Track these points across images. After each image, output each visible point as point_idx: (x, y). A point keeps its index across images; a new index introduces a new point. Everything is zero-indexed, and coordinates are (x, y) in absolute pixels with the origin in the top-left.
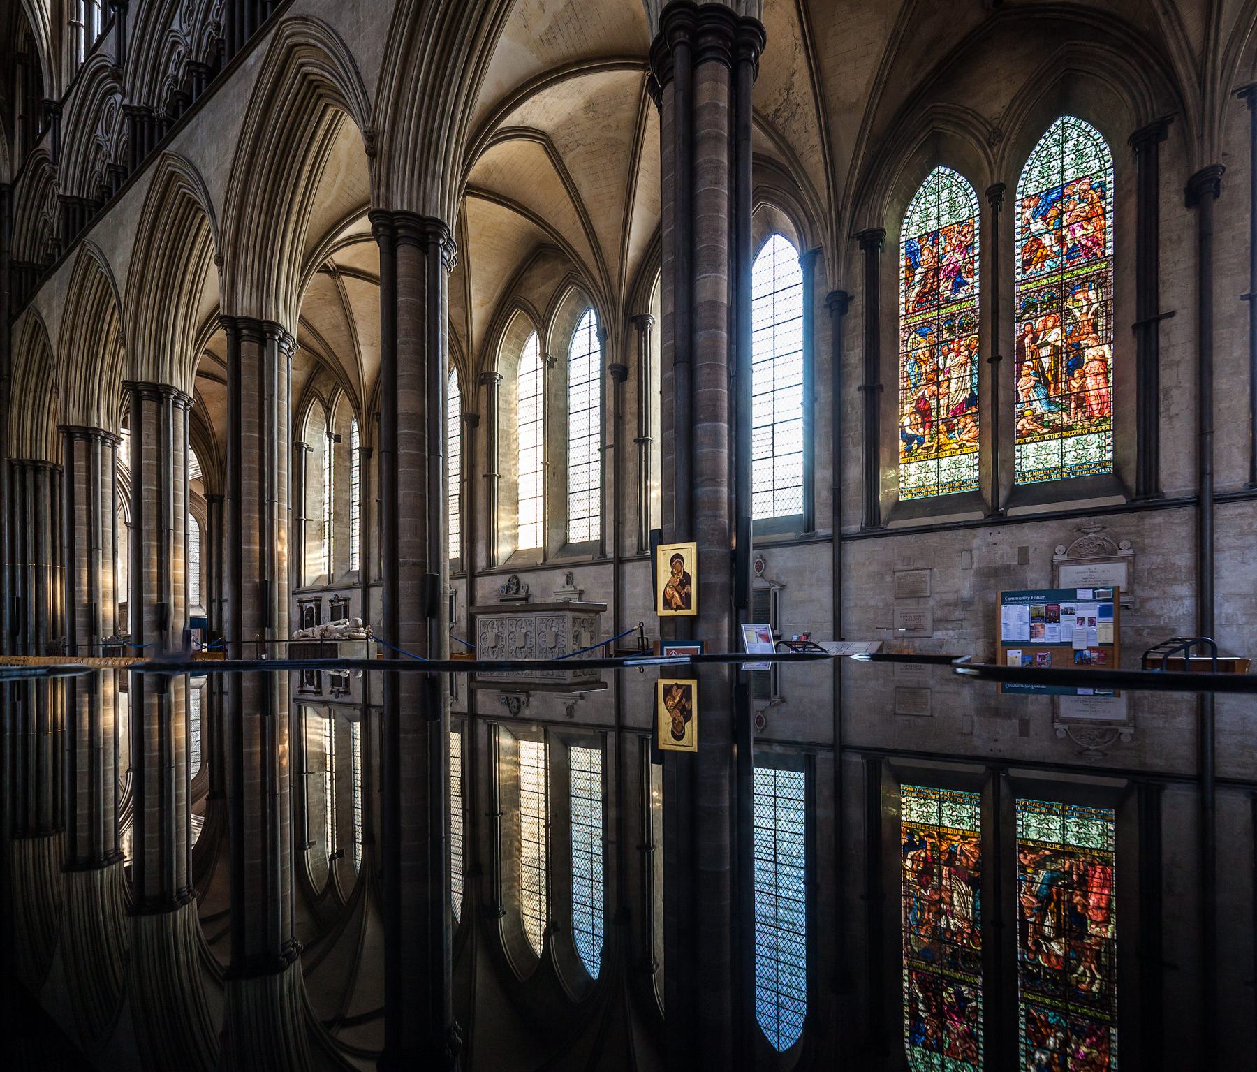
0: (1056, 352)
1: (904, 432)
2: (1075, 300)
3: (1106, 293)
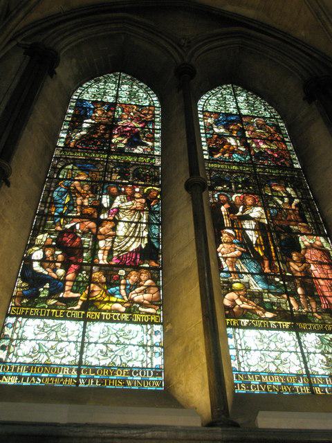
0: (260, 228)
2: (272, 191)
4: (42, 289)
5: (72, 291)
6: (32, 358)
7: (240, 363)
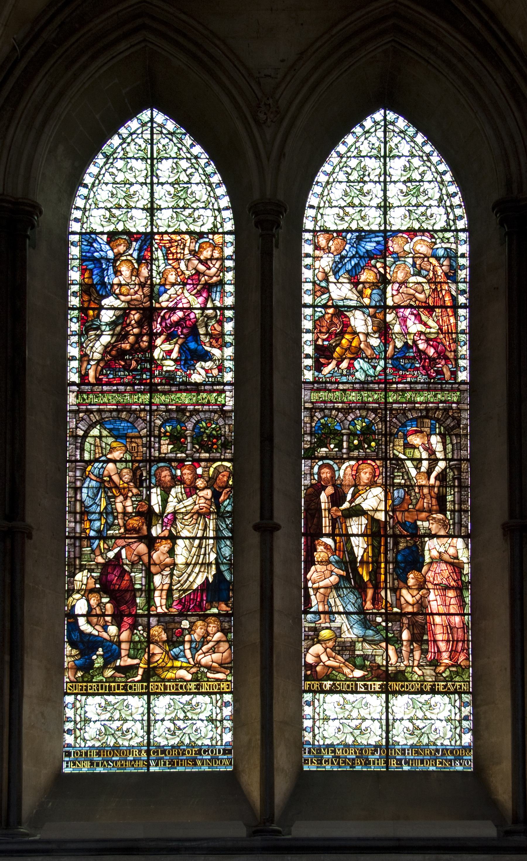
1: (74, 626)
2: (407, 446)
3: (459, 447)
4: (94, 657)
5: (129, 656)
6: (100, 741)
7: (314, 736)
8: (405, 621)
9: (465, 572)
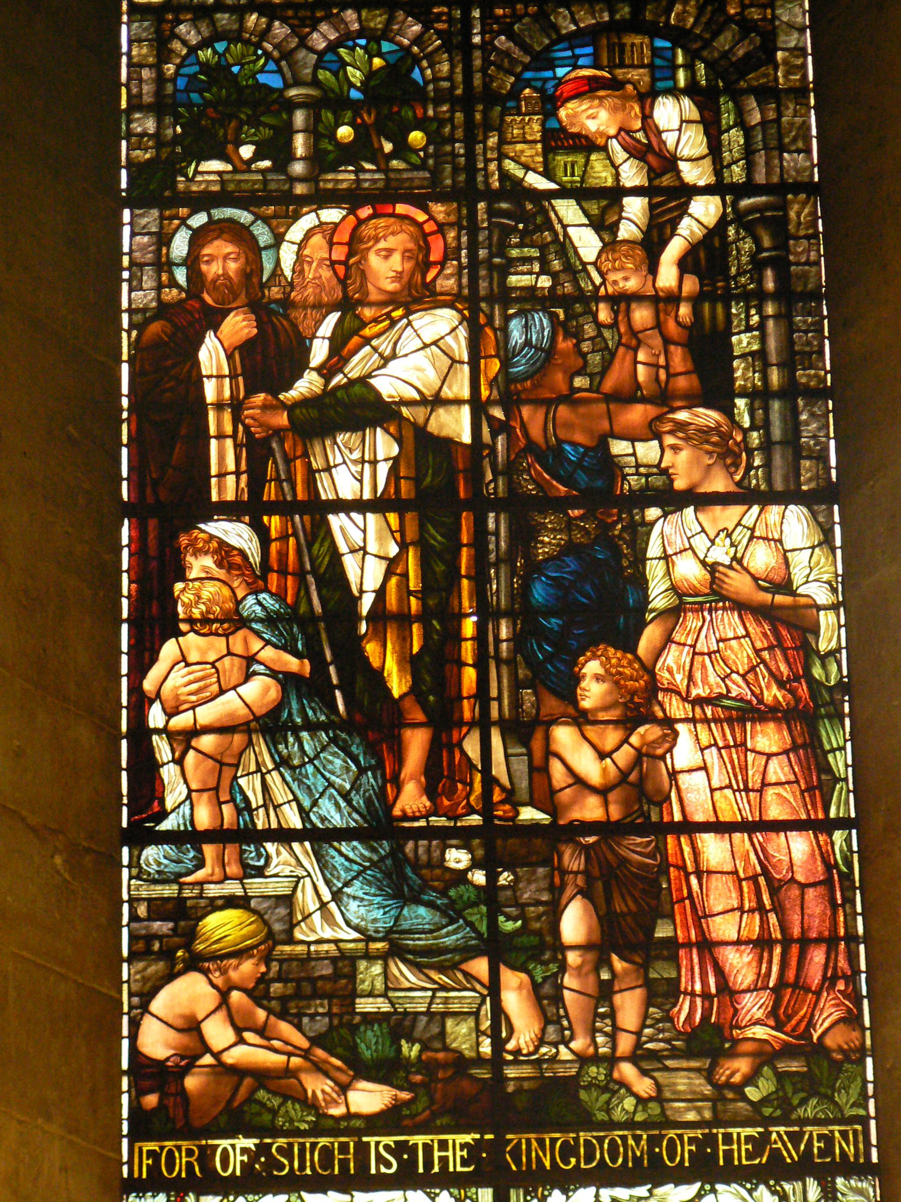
8: (572, 860)
9: (823, 646)
